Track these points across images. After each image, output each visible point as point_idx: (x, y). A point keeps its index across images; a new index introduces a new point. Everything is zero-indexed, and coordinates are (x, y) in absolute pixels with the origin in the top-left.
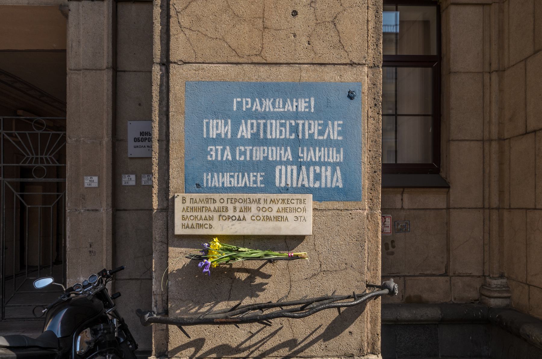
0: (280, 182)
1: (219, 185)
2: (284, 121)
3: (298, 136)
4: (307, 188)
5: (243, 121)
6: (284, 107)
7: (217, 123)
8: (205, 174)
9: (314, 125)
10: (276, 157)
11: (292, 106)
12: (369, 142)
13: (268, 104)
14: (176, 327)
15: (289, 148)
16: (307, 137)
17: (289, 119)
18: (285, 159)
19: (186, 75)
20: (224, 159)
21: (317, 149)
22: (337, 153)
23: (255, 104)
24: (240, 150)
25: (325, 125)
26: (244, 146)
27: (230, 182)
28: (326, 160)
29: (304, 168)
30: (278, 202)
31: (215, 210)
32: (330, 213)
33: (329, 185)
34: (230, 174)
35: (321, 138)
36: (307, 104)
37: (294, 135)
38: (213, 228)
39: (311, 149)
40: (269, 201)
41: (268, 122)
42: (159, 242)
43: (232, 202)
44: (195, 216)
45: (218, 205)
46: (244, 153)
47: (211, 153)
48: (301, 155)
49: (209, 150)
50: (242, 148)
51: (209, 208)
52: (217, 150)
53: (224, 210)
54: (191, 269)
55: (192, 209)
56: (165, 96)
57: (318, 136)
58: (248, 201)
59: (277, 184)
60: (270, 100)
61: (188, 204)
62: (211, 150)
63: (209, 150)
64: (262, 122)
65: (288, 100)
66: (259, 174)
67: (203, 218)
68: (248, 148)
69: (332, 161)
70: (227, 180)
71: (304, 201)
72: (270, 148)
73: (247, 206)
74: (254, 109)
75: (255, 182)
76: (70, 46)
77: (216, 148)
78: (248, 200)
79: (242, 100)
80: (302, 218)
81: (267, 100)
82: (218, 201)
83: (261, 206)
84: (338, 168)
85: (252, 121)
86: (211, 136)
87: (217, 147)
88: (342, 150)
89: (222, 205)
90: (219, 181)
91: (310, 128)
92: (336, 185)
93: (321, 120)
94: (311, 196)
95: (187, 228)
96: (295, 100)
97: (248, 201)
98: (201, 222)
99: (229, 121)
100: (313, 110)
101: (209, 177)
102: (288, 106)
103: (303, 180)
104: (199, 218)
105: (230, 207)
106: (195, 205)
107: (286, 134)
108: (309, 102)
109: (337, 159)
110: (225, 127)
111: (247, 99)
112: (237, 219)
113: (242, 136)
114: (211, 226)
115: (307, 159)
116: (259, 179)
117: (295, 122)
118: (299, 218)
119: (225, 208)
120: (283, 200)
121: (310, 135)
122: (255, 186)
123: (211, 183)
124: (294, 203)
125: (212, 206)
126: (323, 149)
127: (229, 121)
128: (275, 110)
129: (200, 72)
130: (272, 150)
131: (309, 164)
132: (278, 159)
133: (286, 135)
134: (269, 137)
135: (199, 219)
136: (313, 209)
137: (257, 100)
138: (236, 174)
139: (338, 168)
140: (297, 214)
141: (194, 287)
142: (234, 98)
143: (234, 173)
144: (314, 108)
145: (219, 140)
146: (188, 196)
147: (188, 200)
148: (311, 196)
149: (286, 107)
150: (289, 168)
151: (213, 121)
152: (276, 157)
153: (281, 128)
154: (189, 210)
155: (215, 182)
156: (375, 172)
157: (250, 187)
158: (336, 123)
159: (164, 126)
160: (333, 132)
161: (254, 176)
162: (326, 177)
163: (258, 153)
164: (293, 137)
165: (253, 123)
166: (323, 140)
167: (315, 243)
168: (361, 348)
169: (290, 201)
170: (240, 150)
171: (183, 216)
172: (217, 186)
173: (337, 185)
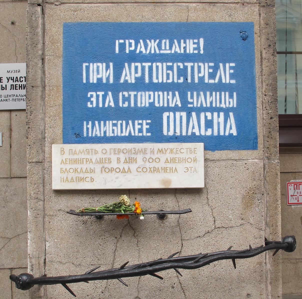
0: (168, 130)
2: (170, 64)
3: (187, 80)
4: (198, 136)
5: (126, 65)
6: (171, 48)
7: (98, 67)
8: (85, 123)
12: (264, 86)
13: (153, 45)
14: (61, 285)
15: (177, 93)
16: (196, 81)
18: (173, 106)
20: (106, 105)
21: (208, 93)
24: (123, 96)
25: (216, 68)
26: (127, 91)
27: (113, 131)
29: (194, 114)
32: (224, 163)
33: (222, 133)
34: (112, 122)
35: (212, 81)
36: (196, 46)
38: (94, 182)
39: (202, 93)
41: (154, 65)
42: (35, 199)
44: (75, 168)
45: (100, 156)
46: (128, 99)
47: (92, 99)
48: (190, 100)
49: (89, 96)
50: (126, 94)
52: (98, 96)
53: (107, 162)
54: (71, 228)
56: (41, 39)
59: (165, 133)
60: (155, 42)
64: (147, 65)
65: (175, 41)
68: (132, 94)
69: (224, 107)
71: (194, 151)
72: (156, 93)
73: (133, 157)
74: (138, 51)
75: (140, 131)
77: (96, 94)
81: (153, 41)
82: (100, 152)
84: (231, 114)
85: (137, 64)
86: (91, 82)
87: (98, 93)
88: (235, 94)
89: (104, 156)
91: (199, 72)
92: (229, 132)
93: (211, 62)
94: (202, 145)
96: (182, 41)
97: (133, 152)
98: (82, 175)
100: (202, 52)
101: (90, 126)
102: (176, 47)
103: (193, 128)
107: (174, 78)
108: (198, 43)
111: (131, 41)
113: (126, 81)
114: (92, 180)
115: (197, 105)
116: (145, 127)
117: (184, 65)
118: (190, 169)
119: (107, 159)
120: (172, 151)
121: (199, 77)
122: (140, 134)
123: (92, 133)
124: (183, 153)
126: (214, 93)
127: (111, 64)
128: (162, 52)
130: (159, 96)
131: (199, 110)
132: (166, 105)
133: (173, 78)
135: (79, 171)
136: (205, 160)
137: (141, 41)
139: (231, 114)
140: (188, 165)
141: (74, 248)
143: (117, 122)
144: (204, 49)
146: (68, 147)
147: (67, 152)
148: (202, 145)
150: (178, 114)
151: (93, 65)
153: (169, 72)
155: (96, 131)
157: (135, 136)
158: (227, 65)
159: (40, 71)
160: (225, 76)
161: (139, 124)
162: (219, 124)
163: (143, 98)
164: (181, 80)
166: (215, 84)
167: (208, 197)
170: (123, 96)
172: (99, 135)
173: (231, 132)
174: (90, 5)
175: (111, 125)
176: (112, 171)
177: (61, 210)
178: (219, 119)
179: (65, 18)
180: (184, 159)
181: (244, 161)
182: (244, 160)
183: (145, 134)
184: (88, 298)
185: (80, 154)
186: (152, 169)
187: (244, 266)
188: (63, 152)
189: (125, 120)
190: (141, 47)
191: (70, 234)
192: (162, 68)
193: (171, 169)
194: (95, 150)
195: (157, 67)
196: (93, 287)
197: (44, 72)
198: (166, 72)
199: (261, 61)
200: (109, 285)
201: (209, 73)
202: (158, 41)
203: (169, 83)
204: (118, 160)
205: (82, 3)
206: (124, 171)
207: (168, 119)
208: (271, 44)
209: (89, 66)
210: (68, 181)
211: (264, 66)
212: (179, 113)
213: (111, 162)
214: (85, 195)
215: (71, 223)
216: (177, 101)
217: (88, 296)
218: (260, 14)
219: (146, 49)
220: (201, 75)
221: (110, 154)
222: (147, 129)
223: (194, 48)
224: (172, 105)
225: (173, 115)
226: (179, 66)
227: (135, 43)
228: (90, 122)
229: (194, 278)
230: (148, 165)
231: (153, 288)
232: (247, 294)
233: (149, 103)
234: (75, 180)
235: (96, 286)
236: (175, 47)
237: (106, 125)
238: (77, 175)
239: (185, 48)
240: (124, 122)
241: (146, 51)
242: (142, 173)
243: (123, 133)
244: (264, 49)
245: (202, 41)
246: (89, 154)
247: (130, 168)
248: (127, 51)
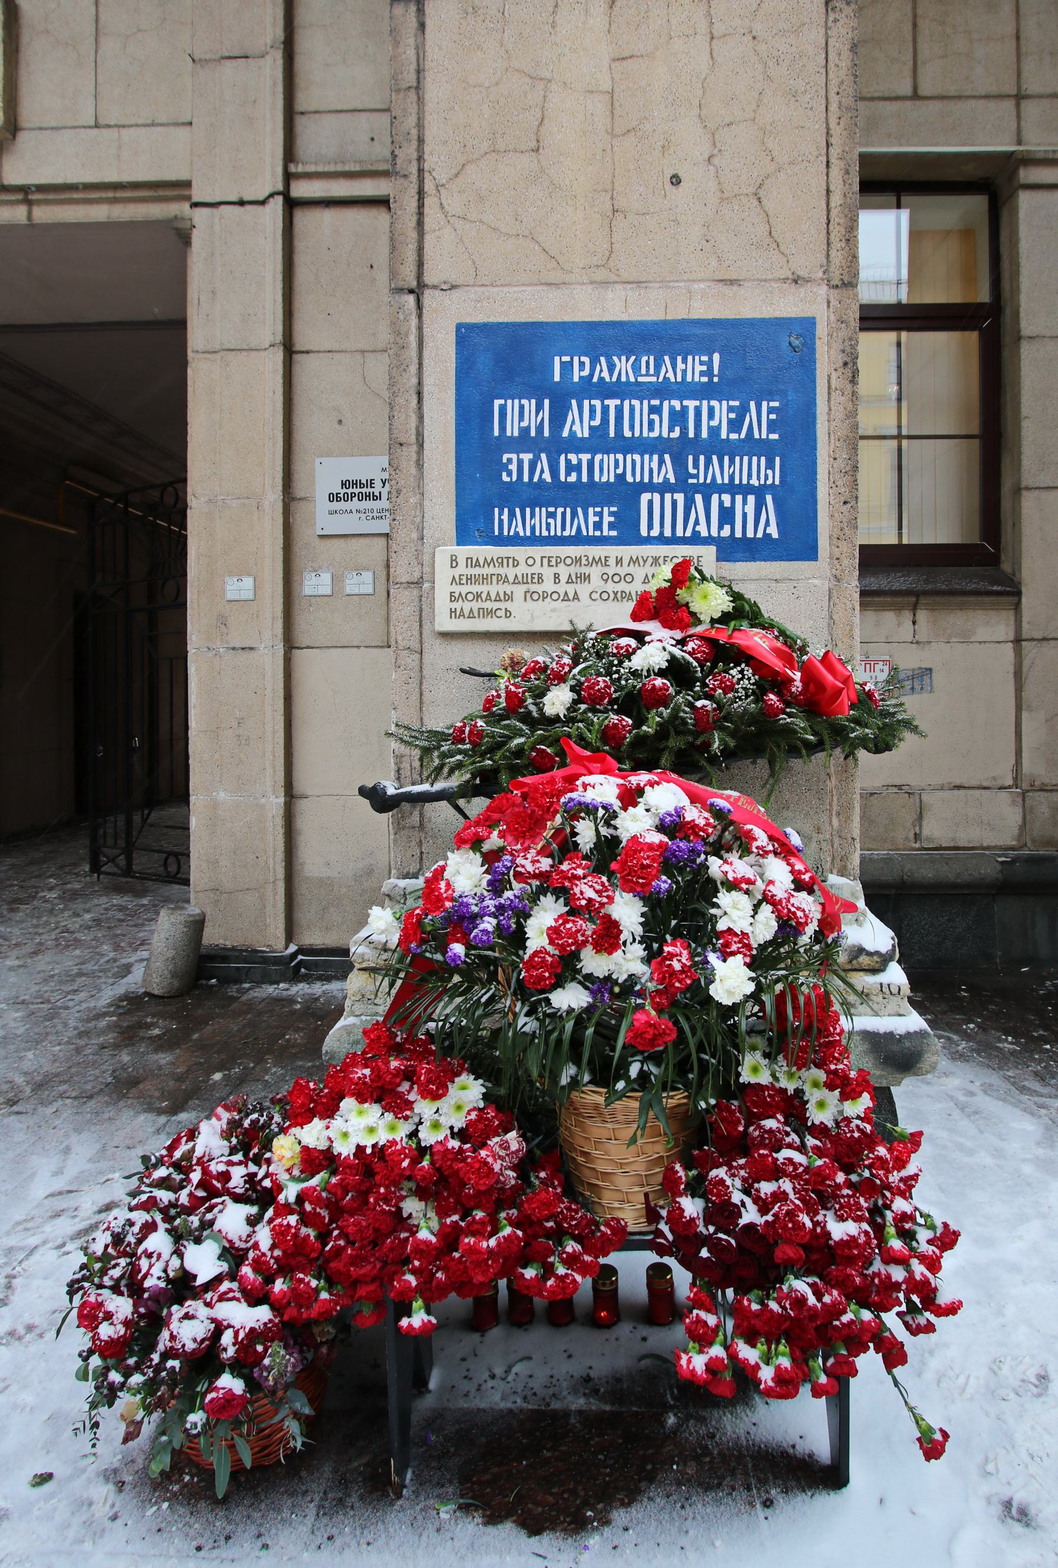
0: (650, 527)
2: (655, 402)
5: (574, 402)
7: (522, 407)
8: (496, 510)
12: (832, 441)
13: (623, 366)
15: (667, 457)
16: (704, 434)
18: (661, 480)
20: (536, 479)
23: (598, 368)
24: (568, 462)
25: (743, 410)
26: (577, 453)
28: (745, 481)
30: (645, 562)
35: (734, 436)
36: (704, 368)
37: (677, 429)
40: (625, 562)
45: (522, 569)
46: (578, 468)
47: (510, 467)
49: (505, 461)
50: (573, 458)
52: (520, 463)
53: (535, 580)
55: (469, 579)
57: (730, 430)
58: (584, 562)
60: (627, 361)
61: (462, 569)
62: (510, 461)
63: (505, 461)
64: (612, 403)
65: (666, 358)
66: (606, 509)
67: (493, 598)
68: (585, 457)
69: (757, 484)
70: (539, 520)
72: (629, 457)
74: (595, 379)
75: (598, 526)
76: (196, 302)
78: (584, 559)
79: (572, 359)
82: (522, 562)
84: (769, 499)
86: (509, 434)
87: (522, 456)
89: (530, 571)
96: (679, 359)
98: (488, 605)
99: (547, 402)
100: (716, 379)
104: (484, 596)
105: (548, 573)
106: (477, 571)
107: (663, 429)
108: (711, 360)
111: (583, 359)
113: (572, 432)
115: (705, 479)
116: (607, 519)
119: (536, 576)
121: (709, 428)
122: (598, 533)
125: (511, 572)
126: (737, 459)
127: (547, 402)
128: (640, 379)
129: (485, 303)
130: (634, 462)
131: (708, 490)
132: (646, 480)
134: (627, 434)
137: (602, 359)
138: (560, 510)
139: (769, 499)
145: (524, 441)
147: (462, 562)
148: (713, 549)
150: (668, 497)
153: (652, 416)
154: (464, 581)
156: (845, 503)
158: (764, 404)
161: (595, 514)
164: (676, 434)
166: (739, 440)
170: (568, 462)
171: (452, 594)
174: (506, 289)
176: (544, 598)
183: (605, 533)
186: (619, 595)
188: (454, 564)
190: (601, 371)
192: (641, 410)
195: (632, 409)
197: (421, 418)
199: (829, 394)
202: (633, 358)
205: (492, 285)
206: (566, 598)
208: (848, 360)
209: (506, 404)
210: (464, 616)
211: (832, 403)
214: (494, 643)
216: (667, 473)
218: (829, 302)
219: (611, 373)
222: (610, 523)
223: (701, 372)
228: (506, 510)
230: (610, 587)
234: (476, 615)
238: (481, 605)
239: (684, 372)
240: (568, 510)
241: (611, 375)
242: (600, 601)
244: (836, 370)
245: (716, 357)
248: (576, 379)
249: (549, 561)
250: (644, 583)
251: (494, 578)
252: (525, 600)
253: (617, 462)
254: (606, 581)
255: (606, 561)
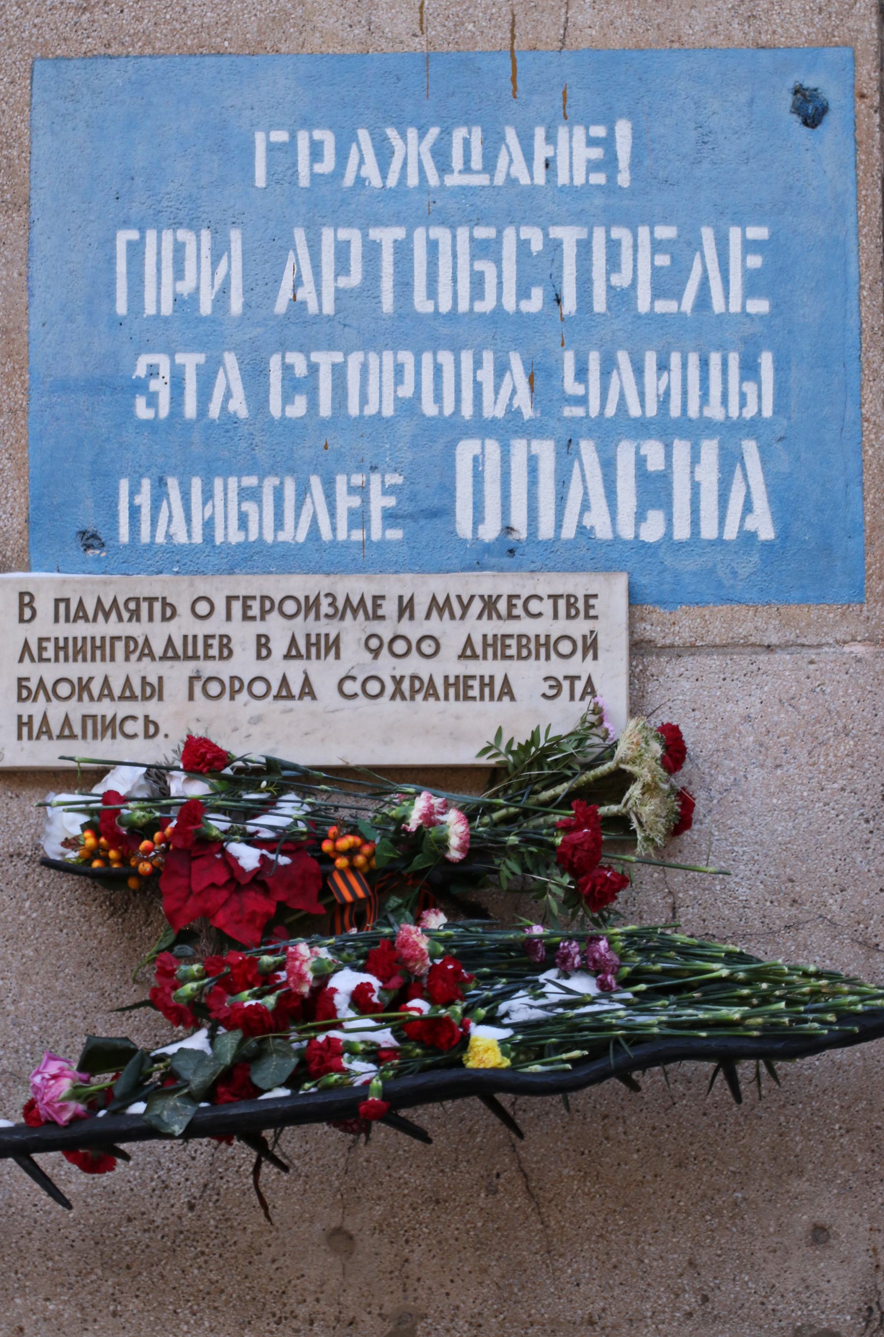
0: (478, 518)
1: (190, 536)
3: (559, 301)
5: (300, 235)
6: (489, 166)
7: (179, 249)
9: (635, 247)
10: (458, 401)
11: (529, 158)
17: (517, 222)
18: (499, 412)
19: (34, 31)
21: (650, 360)
22: (743, 379)
24: (287, 368)
26: (305, 350)
29: (588, 450)
30: (465, 608)
31: (170, 654)
33: (708, 531)
37: (537, 294)
38: (161, 736)
40: (421, 609)
43: (250, 613)
47: (154, 385)
49: (141, 371)
50: (297, 360)
51: (141, 641)
53: (214, 652)
54: (61, 931)
58: (325, 609)
60: (421, 137)
62: (153, 372)
63: (141, 371)
67: (117, 692)
68: (325, 360)
72: (427, 358)
73: (323, 632)
74: (349, 180)
75: (359, 518)
77: (173, 361)
78: (325, 602)
79: (293, 137)
80: (580, 686)
82: (184, 609)
83: (386, 630)
85: (344, 234)
86: (150, 309)
88: (766, 360)
89: (201, 629)
90: (188, 519)
91: (613, 264)
92: (741, 526)
93: (666, 221)
95: (44, 738)
96: (540, 133)
98: (106, 709)
99: (235, 236)
102: (511, 161)
103: (585, 507)
104: (96, 687)
106: (81, 629)
108: (608, 143)
109: (743, 404)
110: (215, 264)
111: (318, 135)
112: (274, 691)
114: (152, 730)
116: (379, 503)
118: (566, 685)
119: (215, 643)
120: (490, 605)
124: (540, 615)
127: (235, 236)
128: (454, 180)
130: (438, 370)
132: (467, 411)
134: (422, 304)
135: (96, 692)
137: (363, 135)
140: (558, 668)
141: (75, 1017)
142: (254, 125)
143: (261, 480)
147: (44, 606)
149: (502, 162)
150: (519, 448)
151: (159, 232)
152: (458, 401)
153: (479, 266)
154: (50, 653)
157: (334, 543)
161: (352, 490)
162: (696, 487)
164: (535, 303)
165: (348, 243)
168: (874, 1306)
169: (519, 603)
170: (287, 368)
171: (21, 682)
175: (233, 495)
177: (19, 855)
178: (697, 469)
179: (41, 40)
180: (542, 640)
181: (805, 650)
182: (803, 645)
183: (376, 534)
184: (130, 1228)
185: (101, 617)
186: (406, 686)
187: (800, 1106)
188: (28, 613)
189: (291, 471)
190: (361, 162)
191: (59, 957)
193: (487, 683)
194: (165, 603)
195: (433, 246)
196: (154, 1184)
198: (467, 267)
200: (222, 1178)
201: (654, 268)
202: (434, 132)
203: (482, 315)
204: (259, 646)
206: (284, 692)
207: (475, 468)
212: (524, 442)
213: (231, 652)
215: (63, 909)
216: (514, 392)
217: (129, 1220)
220: (621, 280)
221: (229, 617)
223: (589, 161)
224: (494, 410)
225: (499, 451)
226: (525, 240)
227: (338, 142)
229: (583, 1153)
231: (406, 1192)
232: (811, 1227)
233: (396, 399)
234: (77, 730)
235: (164, 1178)
236: (507, 158)
237: (211, 497)
241: (384, 177)
242: (362, 700)
243: (282, 530)
245: (623, 130)
246: (138, 620)
247: (312, 679)
248: (304, 181)
249: (246, 608)
250: (462, 656)
251: (120, 646)
252: (191, 697)
253: (399, 370)
254: (376, 653)
255: (376, 606)
